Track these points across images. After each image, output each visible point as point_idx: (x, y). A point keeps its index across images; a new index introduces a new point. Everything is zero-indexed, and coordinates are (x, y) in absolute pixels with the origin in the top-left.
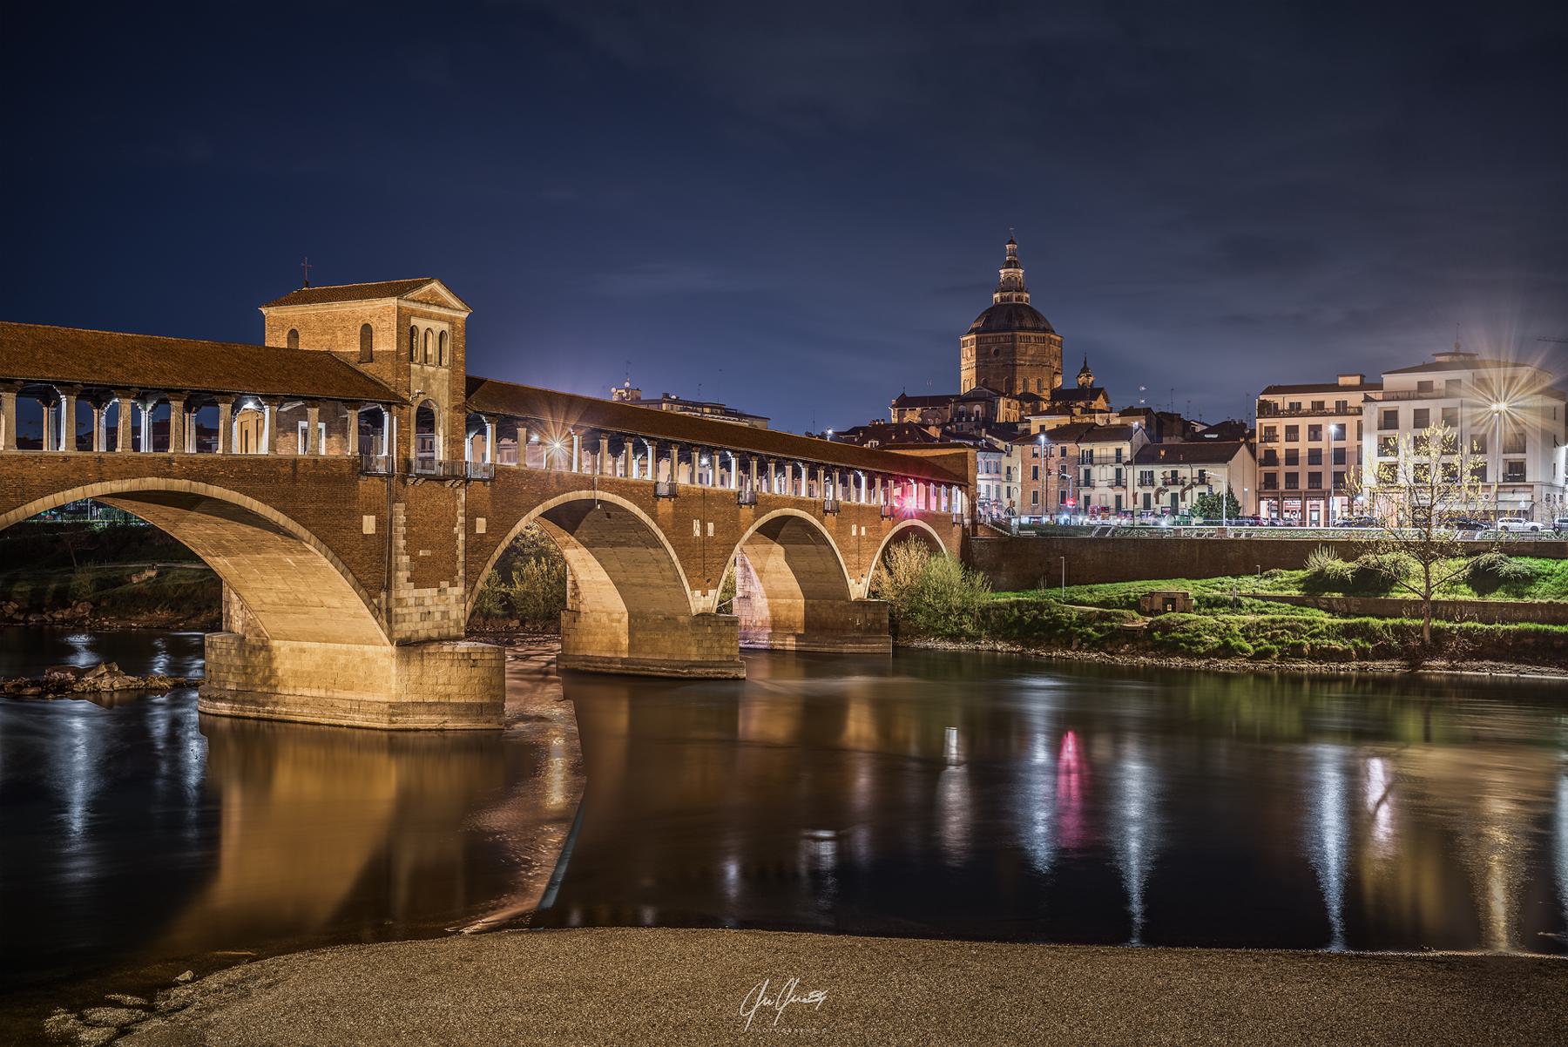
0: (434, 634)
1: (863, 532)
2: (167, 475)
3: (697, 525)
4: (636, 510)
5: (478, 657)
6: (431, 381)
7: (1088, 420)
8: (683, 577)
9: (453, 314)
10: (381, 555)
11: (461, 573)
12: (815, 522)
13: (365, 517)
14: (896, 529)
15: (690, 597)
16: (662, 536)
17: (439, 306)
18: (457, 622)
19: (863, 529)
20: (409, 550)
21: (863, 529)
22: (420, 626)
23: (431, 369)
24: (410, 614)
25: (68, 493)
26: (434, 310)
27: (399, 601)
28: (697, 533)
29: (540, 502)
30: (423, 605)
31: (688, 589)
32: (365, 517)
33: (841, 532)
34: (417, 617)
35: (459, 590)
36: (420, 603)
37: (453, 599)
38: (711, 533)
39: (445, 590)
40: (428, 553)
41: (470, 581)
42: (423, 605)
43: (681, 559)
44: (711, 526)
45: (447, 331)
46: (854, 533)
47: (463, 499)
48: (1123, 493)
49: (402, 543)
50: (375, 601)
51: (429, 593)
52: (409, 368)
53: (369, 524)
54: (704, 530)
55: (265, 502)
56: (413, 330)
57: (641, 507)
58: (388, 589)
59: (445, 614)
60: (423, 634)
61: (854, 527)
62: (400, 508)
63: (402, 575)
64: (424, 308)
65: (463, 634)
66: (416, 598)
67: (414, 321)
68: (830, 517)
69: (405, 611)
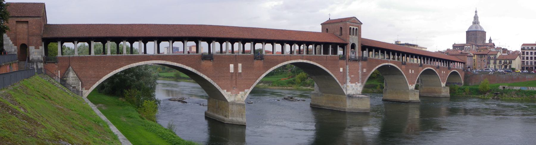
0: (355, 93)
1: (444, 73)
2: (302, 59)
3: (410, 70)
4: (398, 67)
5: (364, 98)
6: (354, 39)
7: (489, 50)
8: (407, 82)
9: (358, 24)
10: (344, 76)
11: (360, 80)
12: (434, 70)
13: (341, 68)
14: (451, 72)
15: (409, 86)
16: (403, 73)
17: (356, 23)
18: (359, 91)
19: (444, 72)
21: (444, 72)
22: (352, 91)
23: (354, 37)
24: (350, 89)
25: (285, 62)
26: (354, 24)
28: (410, 72)
29: (377, 65)
30: (352, 87)
32: (341, 68)
33: (440, 73)
34: (351, 90)
35: (360, 84)
36: (352, 86)
37: (358, 86)
38: (413, 72)
39: (357, 84)
41: (362, 82)
42: (352, 87)
43: (407, 78)
44: (413, 71)
45: (358, 29)
46: (442, 73)
47: (360, 65)
48: (496, 65)
50: (343, 86)
51: (354, 84)
52: (349, 37)
53: (341, 70)
54: (412, 72)
55: (321, 65)
56: (350, 28)
57: (399, 67)
59: (357, 89)
60: (352, 93)
61: (442, 71)
62: (348, 66)
63: (348, 81)
64: (353, 23)
65: (361, 93)
66: (351, 86)
67: (350, 26)
68: (438, 70)
69: (349, 88)
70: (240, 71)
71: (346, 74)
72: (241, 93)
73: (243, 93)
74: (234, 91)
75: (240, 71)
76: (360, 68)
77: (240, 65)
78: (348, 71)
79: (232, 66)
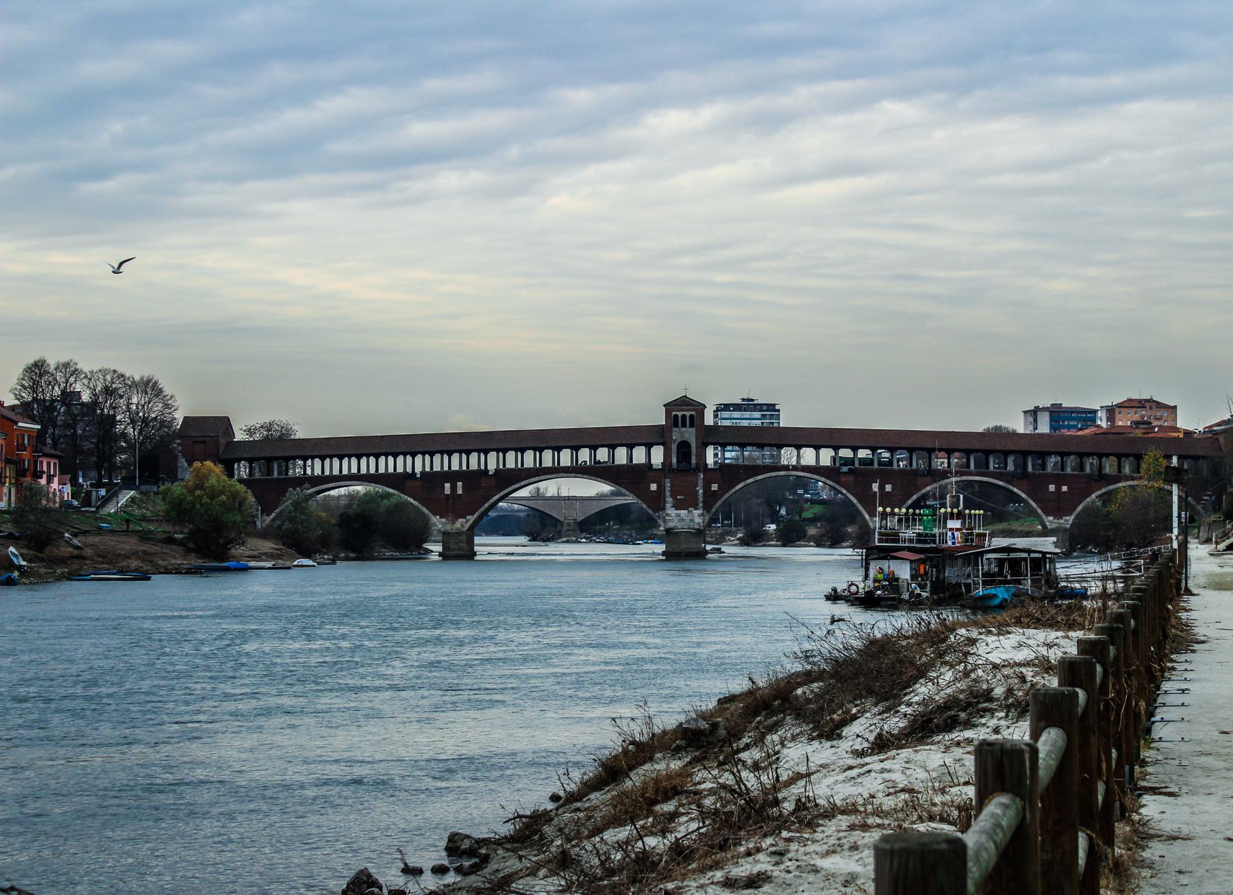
17: (685, 405)
18: (699, 524)
20: (673, 496)
27: (668, 515)
31: (867, 516)
36: (678, 515)
37: (696, 515)
40: (682, 497)
41: (707, 507)
47: (702, 476)
49: (668, 494)
51: (683, 511)
56: (676, 416)
58: (664, 509)
59: (692, 521)
62: (668, 481)
63: (668, 505)
67: (674, 413)
70: (460, 492)
71: (665, 495)
72: (460, 520)
73: (464, 520)
74: (450, 518)
75: (460, 492)
76: (700, 482)
77: (459, 484)
78: (668, 489)
79: (447, 485)
